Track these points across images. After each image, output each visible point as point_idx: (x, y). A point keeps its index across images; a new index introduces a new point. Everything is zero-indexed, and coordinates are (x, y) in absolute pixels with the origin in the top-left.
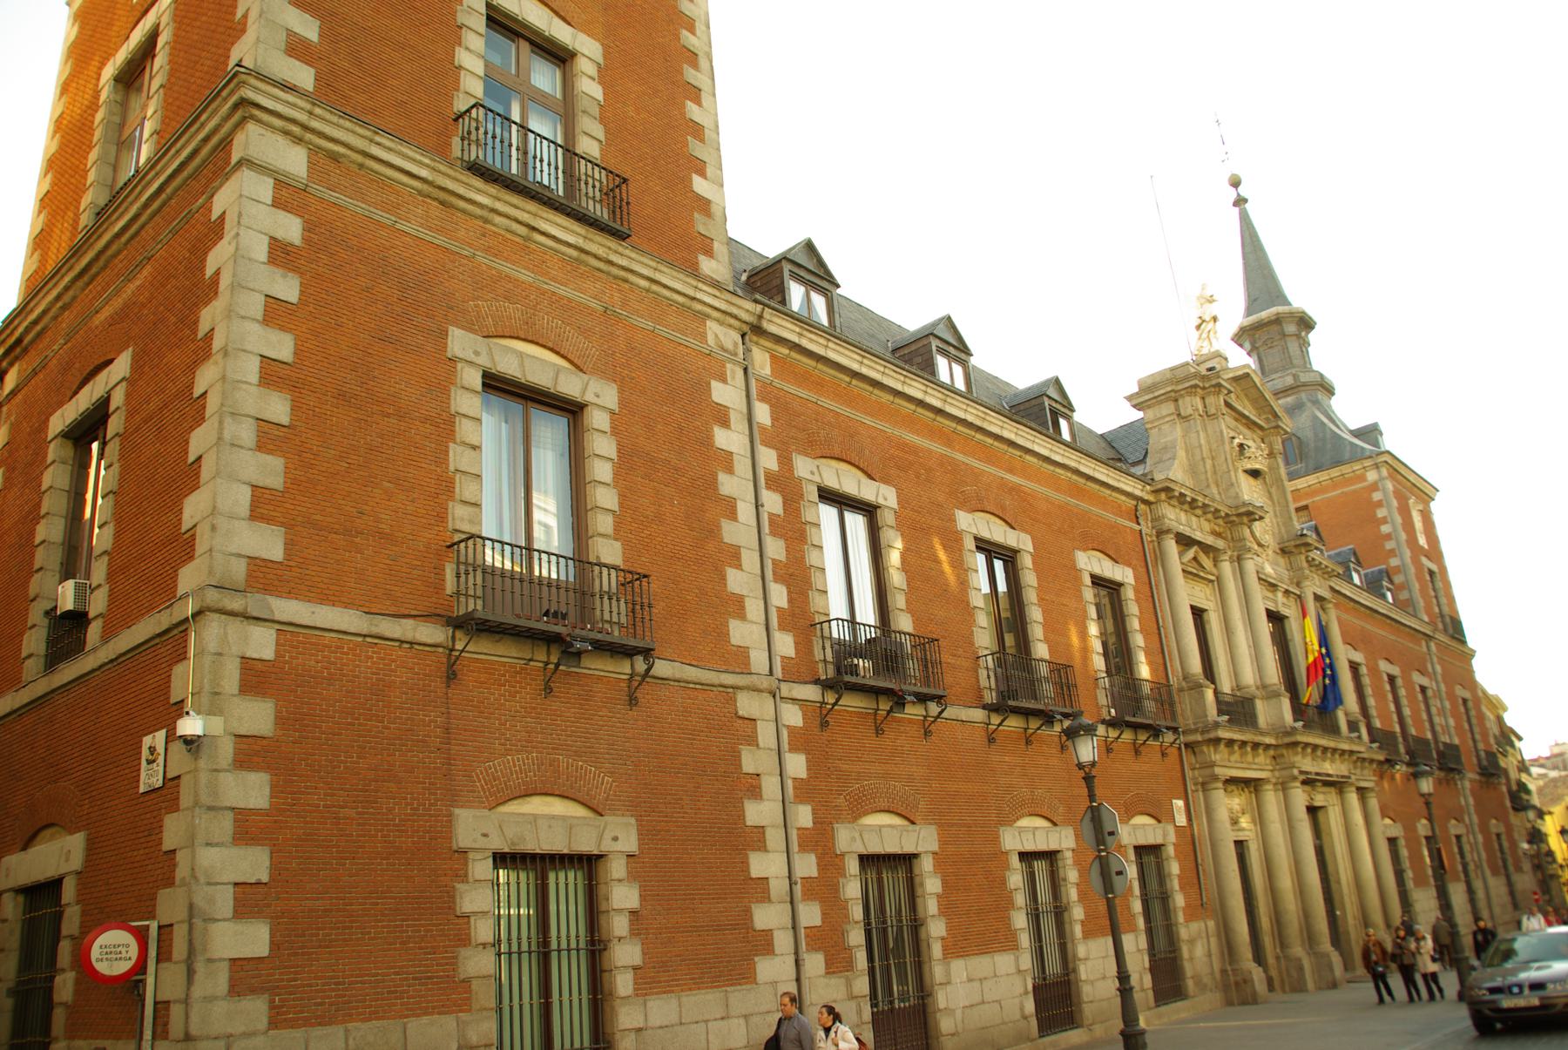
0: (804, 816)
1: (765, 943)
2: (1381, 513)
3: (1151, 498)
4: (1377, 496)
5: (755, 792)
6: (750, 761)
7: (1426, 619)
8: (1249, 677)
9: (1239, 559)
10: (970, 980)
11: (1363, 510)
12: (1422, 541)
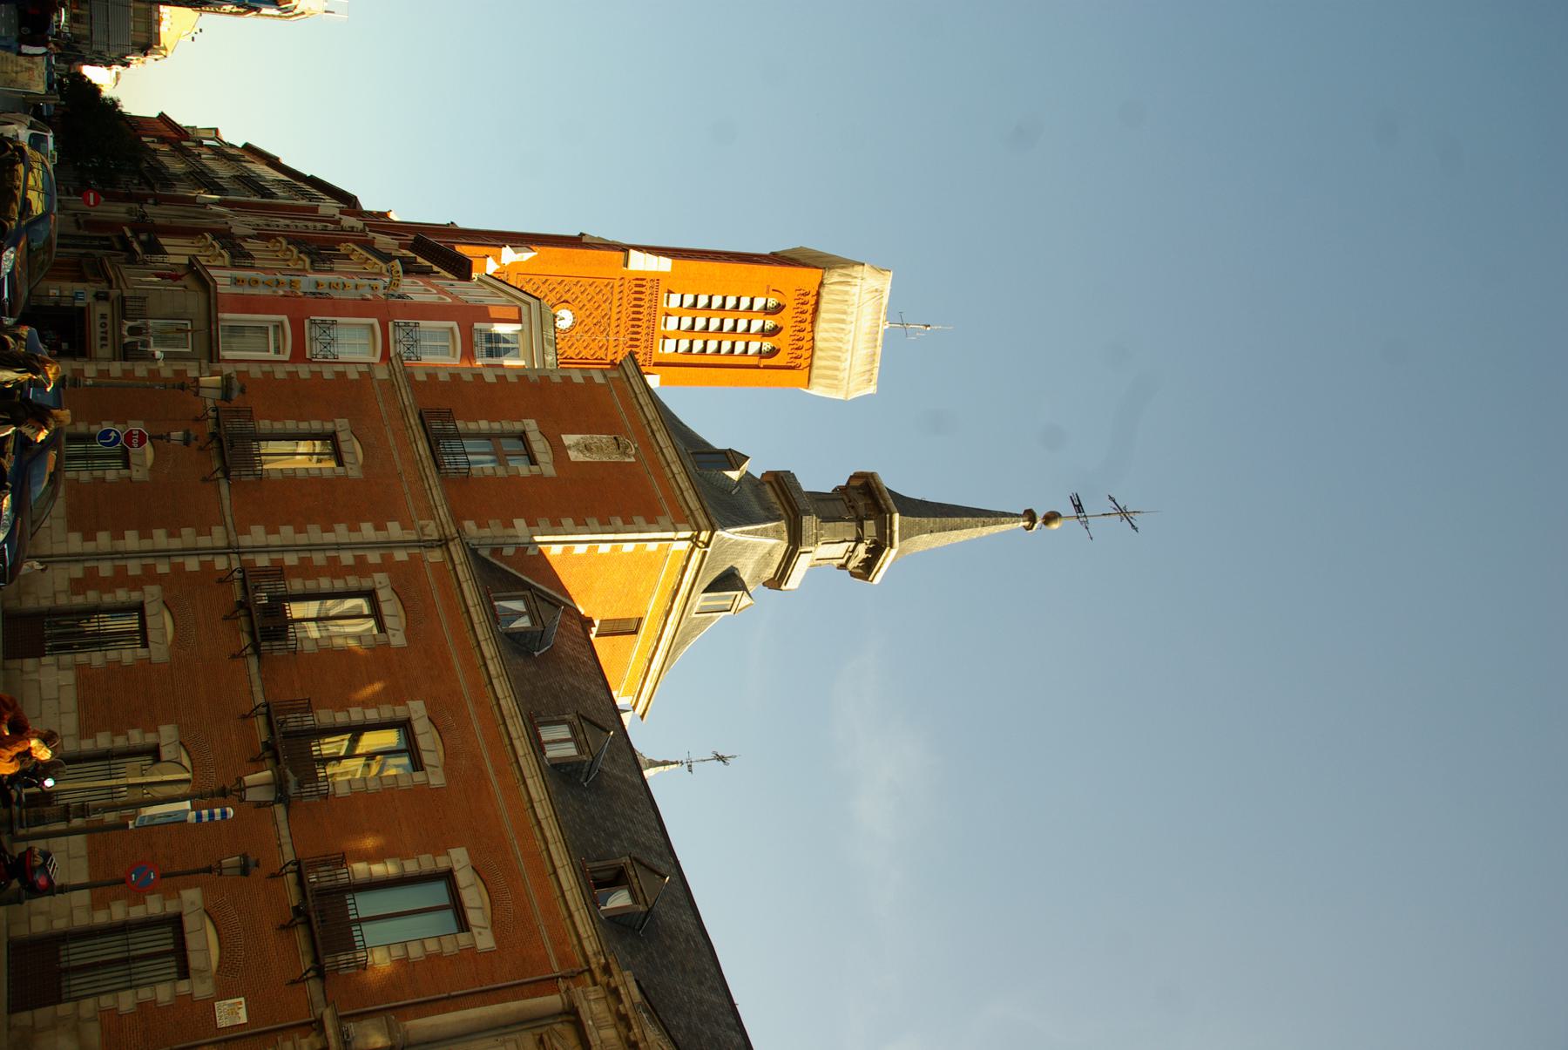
0: (163, 568)
1: (89, 536)
5: (171, 535)
6: (187, 532)
10: (59, 687)
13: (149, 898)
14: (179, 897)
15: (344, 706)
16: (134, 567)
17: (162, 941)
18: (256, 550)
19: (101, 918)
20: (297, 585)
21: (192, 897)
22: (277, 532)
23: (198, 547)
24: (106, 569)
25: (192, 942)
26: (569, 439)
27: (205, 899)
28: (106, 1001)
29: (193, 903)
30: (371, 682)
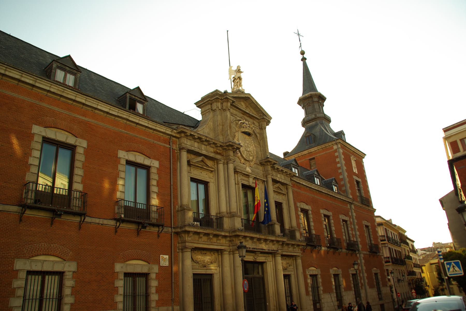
2: (338, 160)
3: (178, 136)
4: (336, 154)
7: (351, 197)
8: (224, 209)
9: (227, 163)
11: (331, 159)
12: (355, 170)
14: (118, 272)
21: (119, 267)
29: (122, 267)
30: (11, 144)
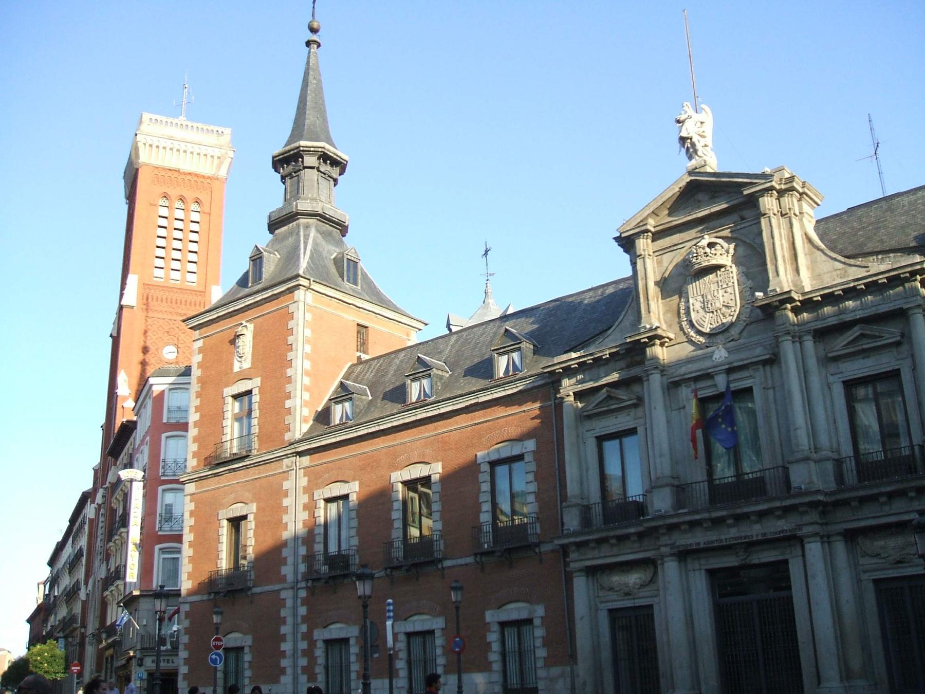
0: (304, 628)
1: (283, 671)
5: (284, 623)
6: (283, 613)
13: (488, 640)
14: (489, 623)
15: (390, 522)
16: (303, 645)
17: (511, 633)
18: (296, 572)
19: (497, 667)
20: (319, 548)
21: (490, 616)
22: (285, 559)
23: (293, 608)
24: (303, 662)
25: (514, 616)
26: (236, 368)
27: (491, 609)
28: (540, 663)
